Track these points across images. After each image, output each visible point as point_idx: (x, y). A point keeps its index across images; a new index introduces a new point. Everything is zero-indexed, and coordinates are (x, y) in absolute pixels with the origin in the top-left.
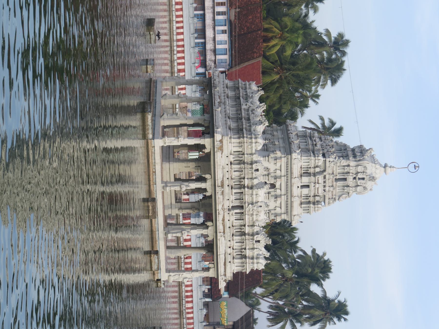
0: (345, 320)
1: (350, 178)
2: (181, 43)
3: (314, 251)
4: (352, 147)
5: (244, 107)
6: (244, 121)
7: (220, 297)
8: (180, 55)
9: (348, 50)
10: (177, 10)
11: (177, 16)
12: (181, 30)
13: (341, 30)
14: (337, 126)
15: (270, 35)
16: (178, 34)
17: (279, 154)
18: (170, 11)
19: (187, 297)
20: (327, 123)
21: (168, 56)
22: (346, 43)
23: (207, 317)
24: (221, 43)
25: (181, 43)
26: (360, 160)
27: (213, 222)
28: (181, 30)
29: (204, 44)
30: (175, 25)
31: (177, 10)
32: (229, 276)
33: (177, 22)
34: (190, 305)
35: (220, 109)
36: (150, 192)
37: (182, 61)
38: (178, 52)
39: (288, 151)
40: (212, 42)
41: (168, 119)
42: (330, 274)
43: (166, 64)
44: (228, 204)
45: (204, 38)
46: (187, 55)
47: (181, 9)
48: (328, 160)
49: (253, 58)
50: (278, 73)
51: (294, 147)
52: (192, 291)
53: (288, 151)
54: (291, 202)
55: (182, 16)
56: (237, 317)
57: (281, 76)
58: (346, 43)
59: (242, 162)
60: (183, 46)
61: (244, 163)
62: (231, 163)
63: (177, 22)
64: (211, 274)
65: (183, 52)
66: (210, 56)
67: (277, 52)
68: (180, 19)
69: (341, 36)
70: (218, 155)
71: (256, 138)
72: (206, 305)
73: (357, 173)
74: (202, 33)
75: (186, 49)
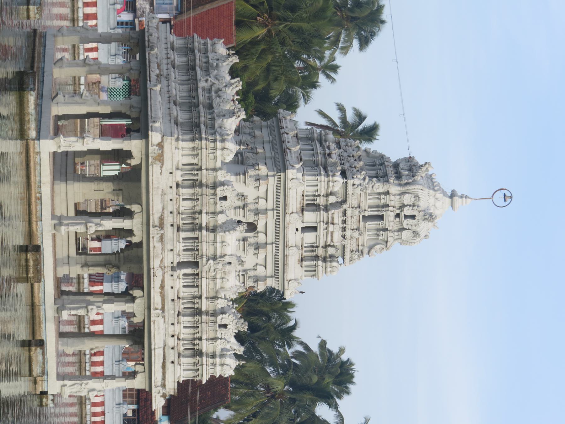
1: (389, 216)
3: (323, 345)
4: (393, 160)
5: (202, 84)
6: (202, 110)
14: (367, 123)
17: (263, 170)
20: (350, 117)
26: (407, 184)
27: (143, 289)
32: (171, 388)
35: (158, 88)
36: (30, 234)
41: (66, 103)
42: (351, 386)
44: (170, 258)
48: (350, 182)
50: (264, 25)
51: (291, 157)
52: (103, 414)
54: (285, 256)
57: (269, 31)
59: (196, 184)
61: (201, 185)
62: (178, 185)
64: (139, 383)
70: (155, 169)
71: (223, 141)
73: (403, 206)
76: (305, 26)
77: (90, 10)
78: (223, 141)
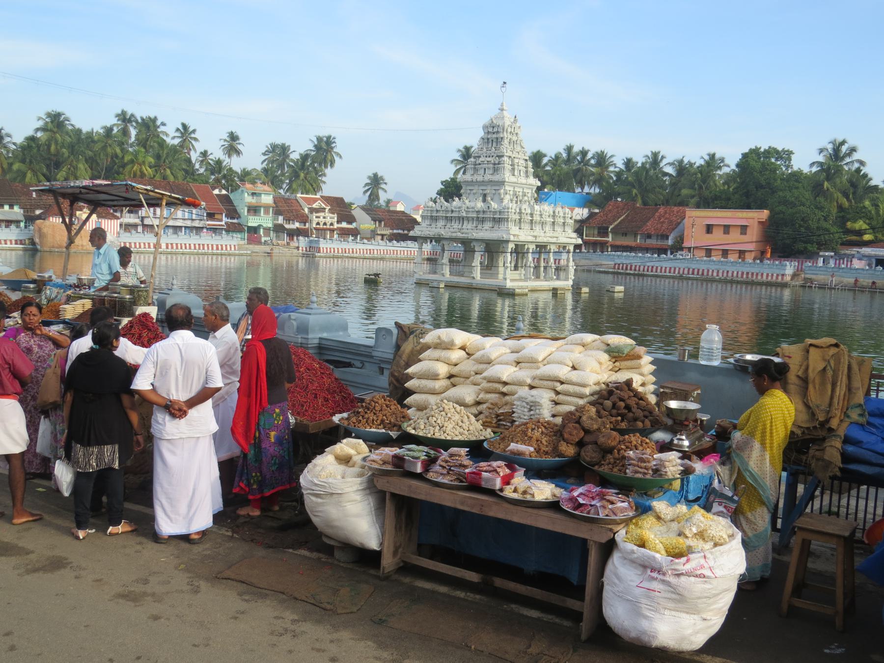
0: (334, 138)
1: (514, 138)
2: (197, 246)
4: (483, 133)
5: (464, 214)
6: (485, 216)
7: (356, 229)
8: (206, 248)
9: (129, 113)
10: (172, 248)
11: (195, 248)
12: (188, 245)
13: (113, 116)
14: (180, 127)
15: (138, 173)
16: (190, 248)
17: (502, 191)
18: (176, 254)
19: (370, 253)
20: (178, 134)
21: (224, 257)
22: (124, 113)
23: (369, 239)
24: (184, 215)
25: (197, 246)
26: (503, 130)
28: (188, 245)
29: (186, 227)
30: (142, 249)
31: (172, 248)
32: (574, 235)
33: (177, 248)
34: (376, 251)
36: (550, 290)
37: (210, 246)
38: (204, 249)
39: (502, 183)
40: (186, 222)
42: (286, 145)
43: (185, 258)
44: (542, 234)
45: (181, 227)
46: (206, 242)
47: (172, 244)
49: (192, 189)
50: (165, 169)
51: (496, 178)
53: (502, 183)
55: (177, 244)
56: (368, 218)
58: (124, 113)
60: (199, 245)
61: (520, 220)
62: (520, 229)
63: (177, 248)
64: (572, 248)
65: (203, 245)
66: (196, 224)
67: (150, 167)
68: (174, 245)
69: (117, 116)
70: (539, 240)
71: (508, 208)
72: (362, 239)
74: (177, 229)
75: (201, 242)
76: (165, 152)
77: (215, 248)
78: (508, 208)
